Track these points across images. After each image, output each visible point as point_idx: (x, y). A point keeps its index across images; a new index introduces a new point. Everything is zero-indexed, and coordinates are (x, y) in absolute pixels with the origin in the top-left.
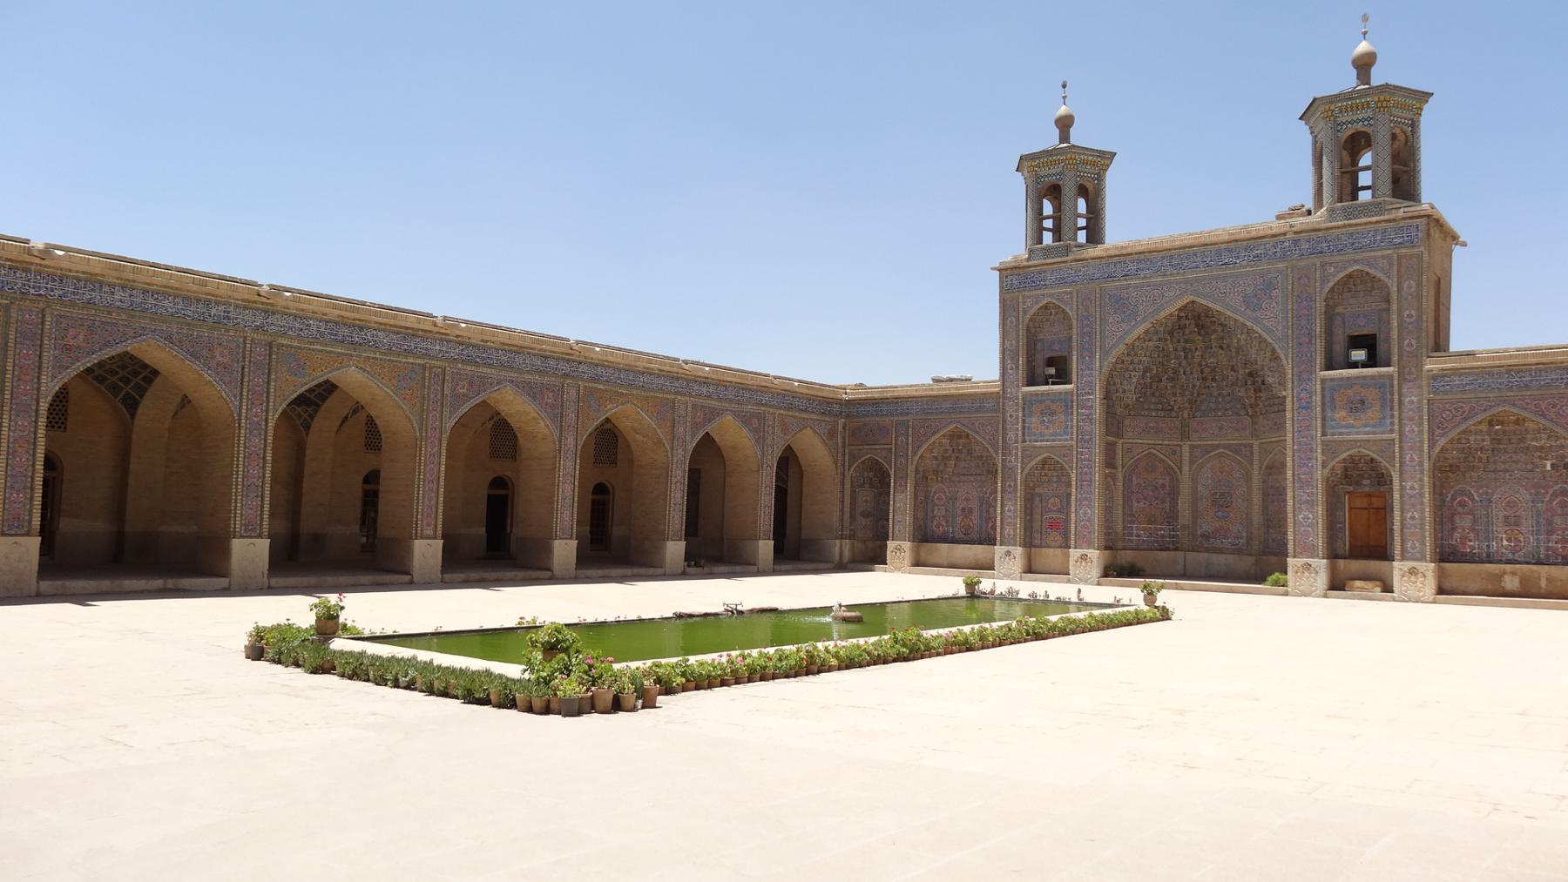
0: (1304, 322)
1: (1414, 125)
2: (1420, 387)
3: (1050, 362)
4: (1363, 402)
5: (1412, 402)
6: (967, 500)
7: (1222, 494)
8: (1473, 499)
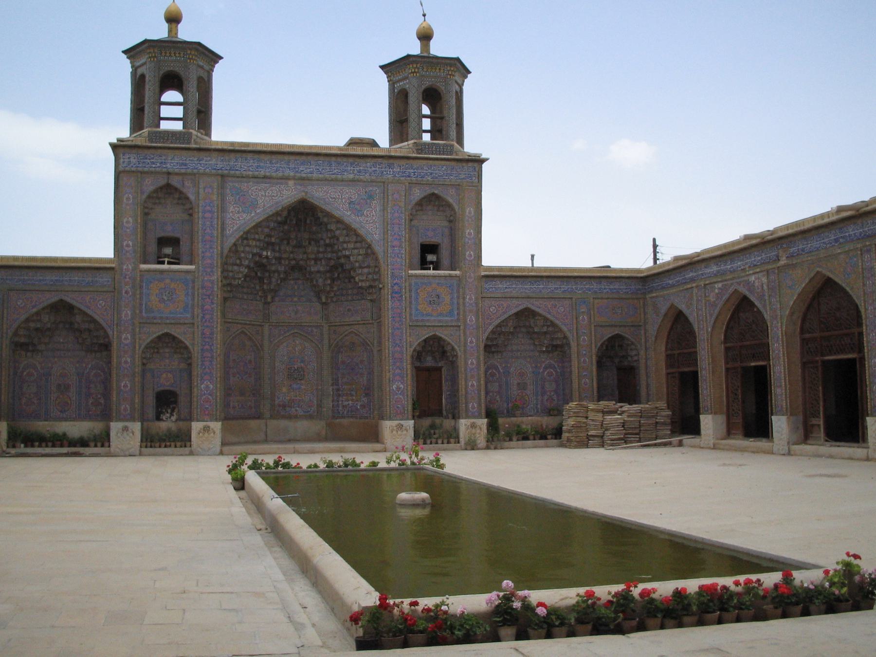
3: (163, 242)
4: (438, 296)
8: (499, 372)
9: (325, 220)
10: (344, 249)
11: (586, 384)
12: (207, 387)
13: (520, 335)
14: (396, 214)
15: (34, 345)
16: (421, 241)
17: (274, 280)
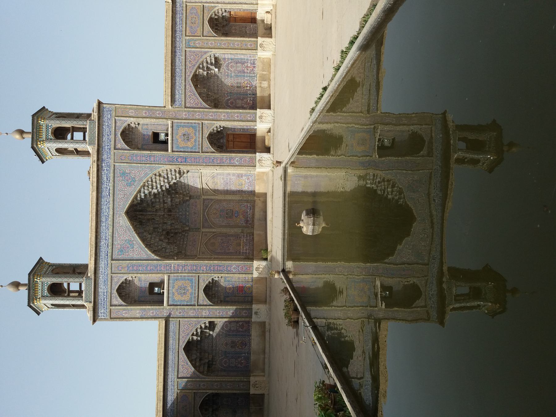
0: (144, 159)
1: (56, 114)
2: (179, 111)
5: (186, 115)
6: (226, 344)
7: (227, 214)
9: (139, 199)
10: (157, 188)
11: (238, 45)
12: (234, 268)
13: (209, 84)
14: (134, 158)
15: (209, 361)
16: (151, 143)
17: (176, 227)
